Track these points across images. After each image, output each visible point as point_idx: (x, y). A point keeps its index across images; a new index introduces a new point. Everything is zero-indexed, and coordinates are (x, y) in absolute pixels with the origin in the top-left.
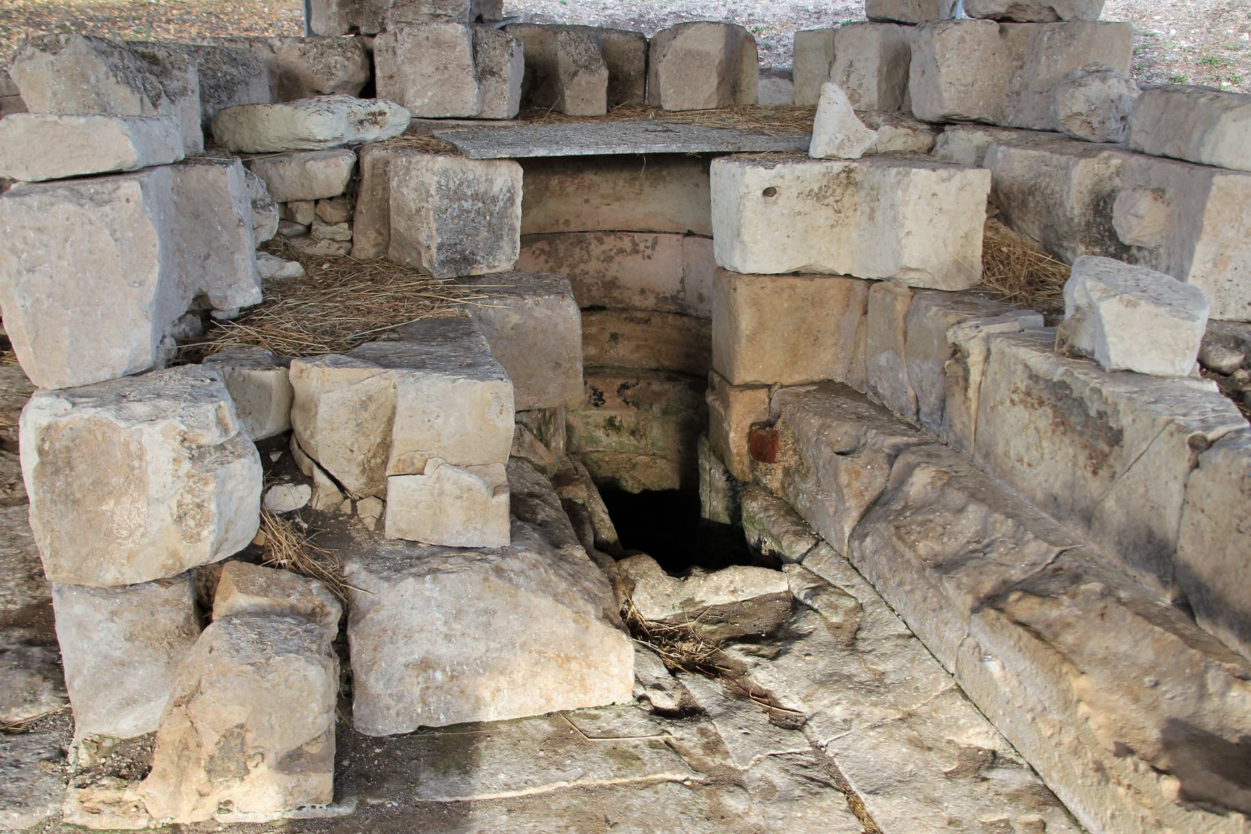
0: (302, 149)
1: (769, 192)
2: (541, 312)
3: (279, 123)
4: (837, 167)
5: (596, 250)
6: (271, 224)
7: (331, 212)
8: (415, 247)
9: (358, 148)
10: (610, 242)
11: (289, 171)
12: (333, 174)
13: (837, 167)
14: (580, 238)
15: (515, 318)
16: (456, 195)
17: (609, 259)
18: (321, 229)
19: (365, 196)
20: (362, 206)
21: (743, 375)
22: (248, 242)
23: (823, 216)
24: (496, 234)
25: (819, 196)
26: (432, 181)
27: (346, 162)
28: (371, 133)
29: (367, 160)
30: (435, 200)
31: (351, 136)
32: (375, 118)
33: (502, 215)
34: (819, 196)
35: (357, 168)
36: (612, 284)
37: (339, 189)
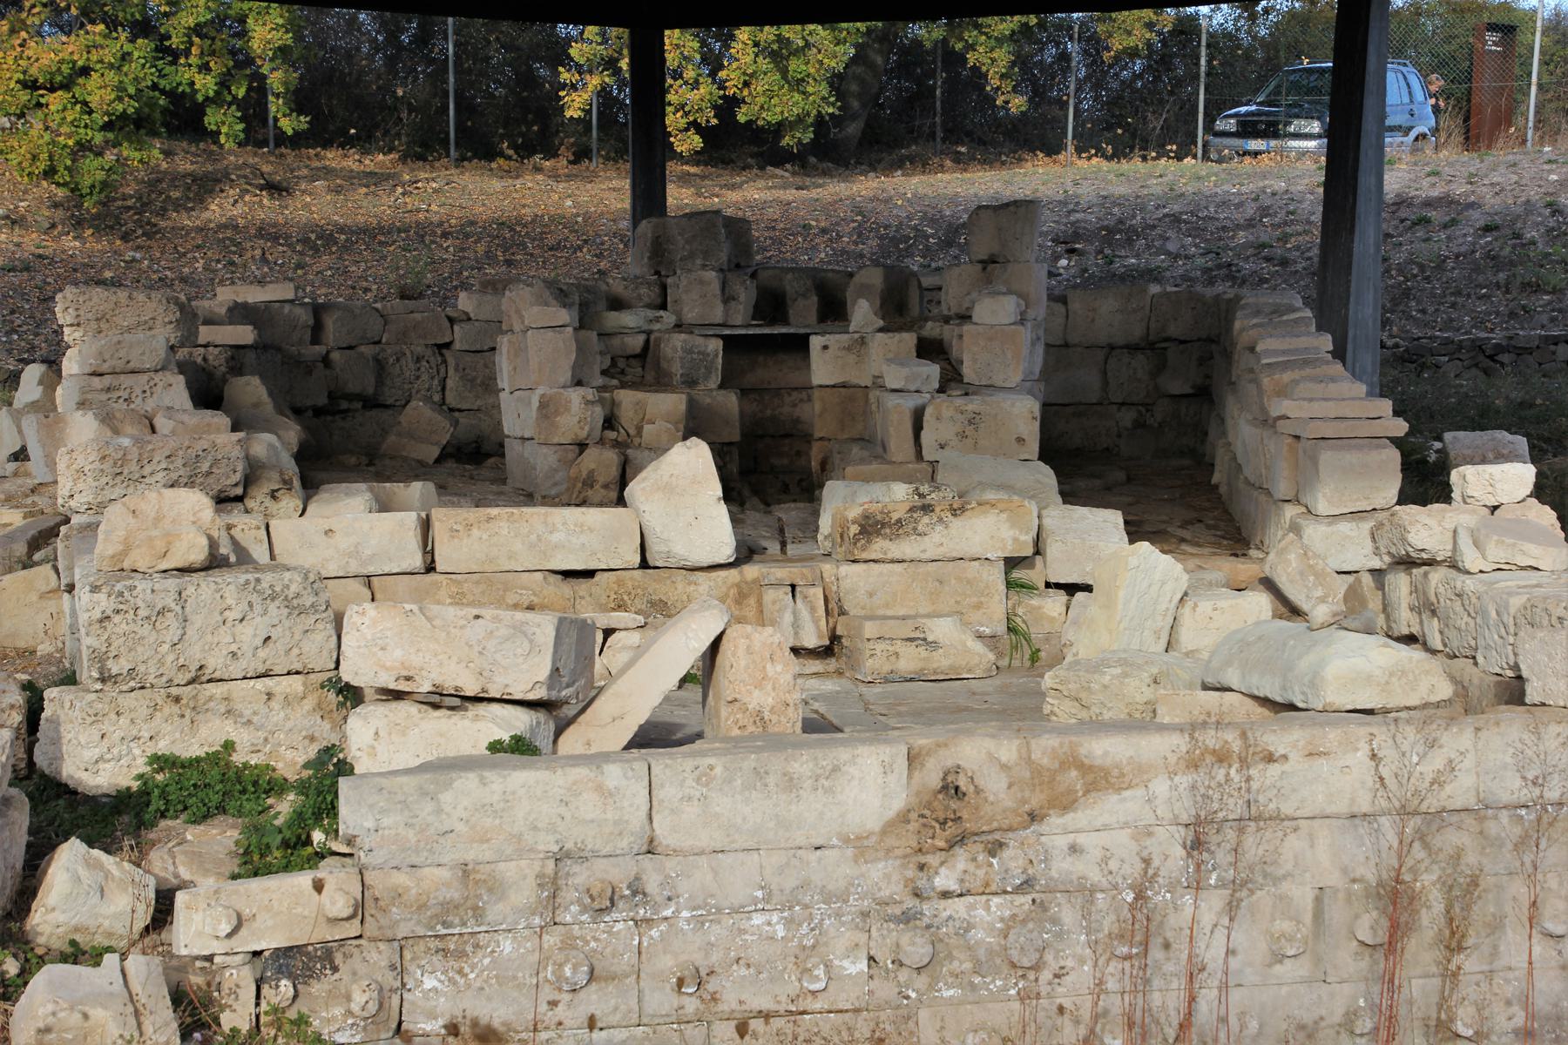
0: (621, 332)
1: (825, 347)
2: (720, 398)
3: (615, 319)
4: (856, 336)
5: (787, 399)
6: (608, 362)
7: (633, 362)
8: (670, 375)
9: (649, 333)
10: (795, 394)
11: (616, 341)
12: (637, 343)
13: (856, 336)
14: (777, 392)
15: (708, 400)
16: (690, 352)
17: (795, 405)
18: (628, 370)
19: (650, 355)
20: (649, 359)
21: (817, 435)
22: (597, 370)
23: (852, 358)
24: (709, 370)
25: (849, 349)
26: (679, 345)
27: (641, 338)
28: (657, 326)
29: (652, 337)
30: (680, 353)
31: (646, 327)
32: (658, 319)
33: (713, 362)
34: (849, 349)
35: (647, 341)
36: (797, 421)
37: (638, 350)
